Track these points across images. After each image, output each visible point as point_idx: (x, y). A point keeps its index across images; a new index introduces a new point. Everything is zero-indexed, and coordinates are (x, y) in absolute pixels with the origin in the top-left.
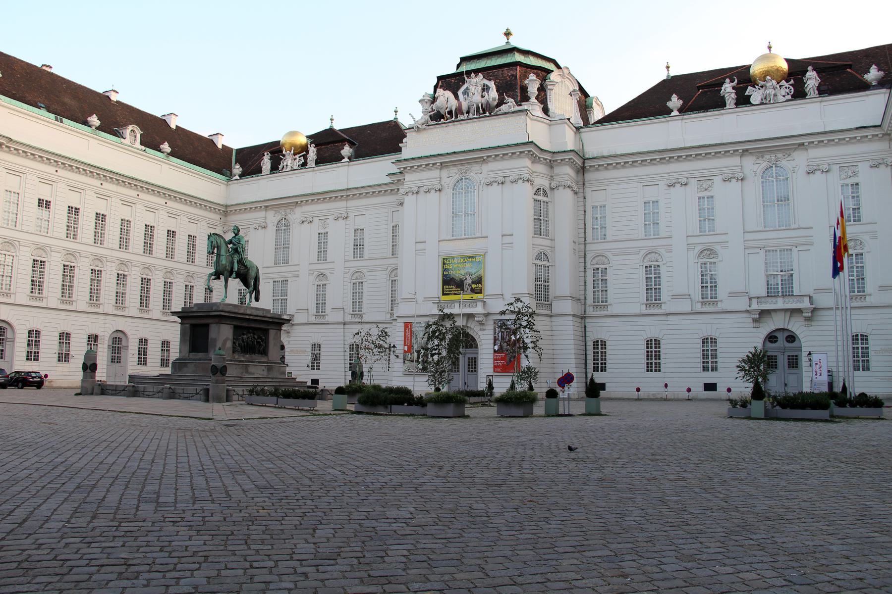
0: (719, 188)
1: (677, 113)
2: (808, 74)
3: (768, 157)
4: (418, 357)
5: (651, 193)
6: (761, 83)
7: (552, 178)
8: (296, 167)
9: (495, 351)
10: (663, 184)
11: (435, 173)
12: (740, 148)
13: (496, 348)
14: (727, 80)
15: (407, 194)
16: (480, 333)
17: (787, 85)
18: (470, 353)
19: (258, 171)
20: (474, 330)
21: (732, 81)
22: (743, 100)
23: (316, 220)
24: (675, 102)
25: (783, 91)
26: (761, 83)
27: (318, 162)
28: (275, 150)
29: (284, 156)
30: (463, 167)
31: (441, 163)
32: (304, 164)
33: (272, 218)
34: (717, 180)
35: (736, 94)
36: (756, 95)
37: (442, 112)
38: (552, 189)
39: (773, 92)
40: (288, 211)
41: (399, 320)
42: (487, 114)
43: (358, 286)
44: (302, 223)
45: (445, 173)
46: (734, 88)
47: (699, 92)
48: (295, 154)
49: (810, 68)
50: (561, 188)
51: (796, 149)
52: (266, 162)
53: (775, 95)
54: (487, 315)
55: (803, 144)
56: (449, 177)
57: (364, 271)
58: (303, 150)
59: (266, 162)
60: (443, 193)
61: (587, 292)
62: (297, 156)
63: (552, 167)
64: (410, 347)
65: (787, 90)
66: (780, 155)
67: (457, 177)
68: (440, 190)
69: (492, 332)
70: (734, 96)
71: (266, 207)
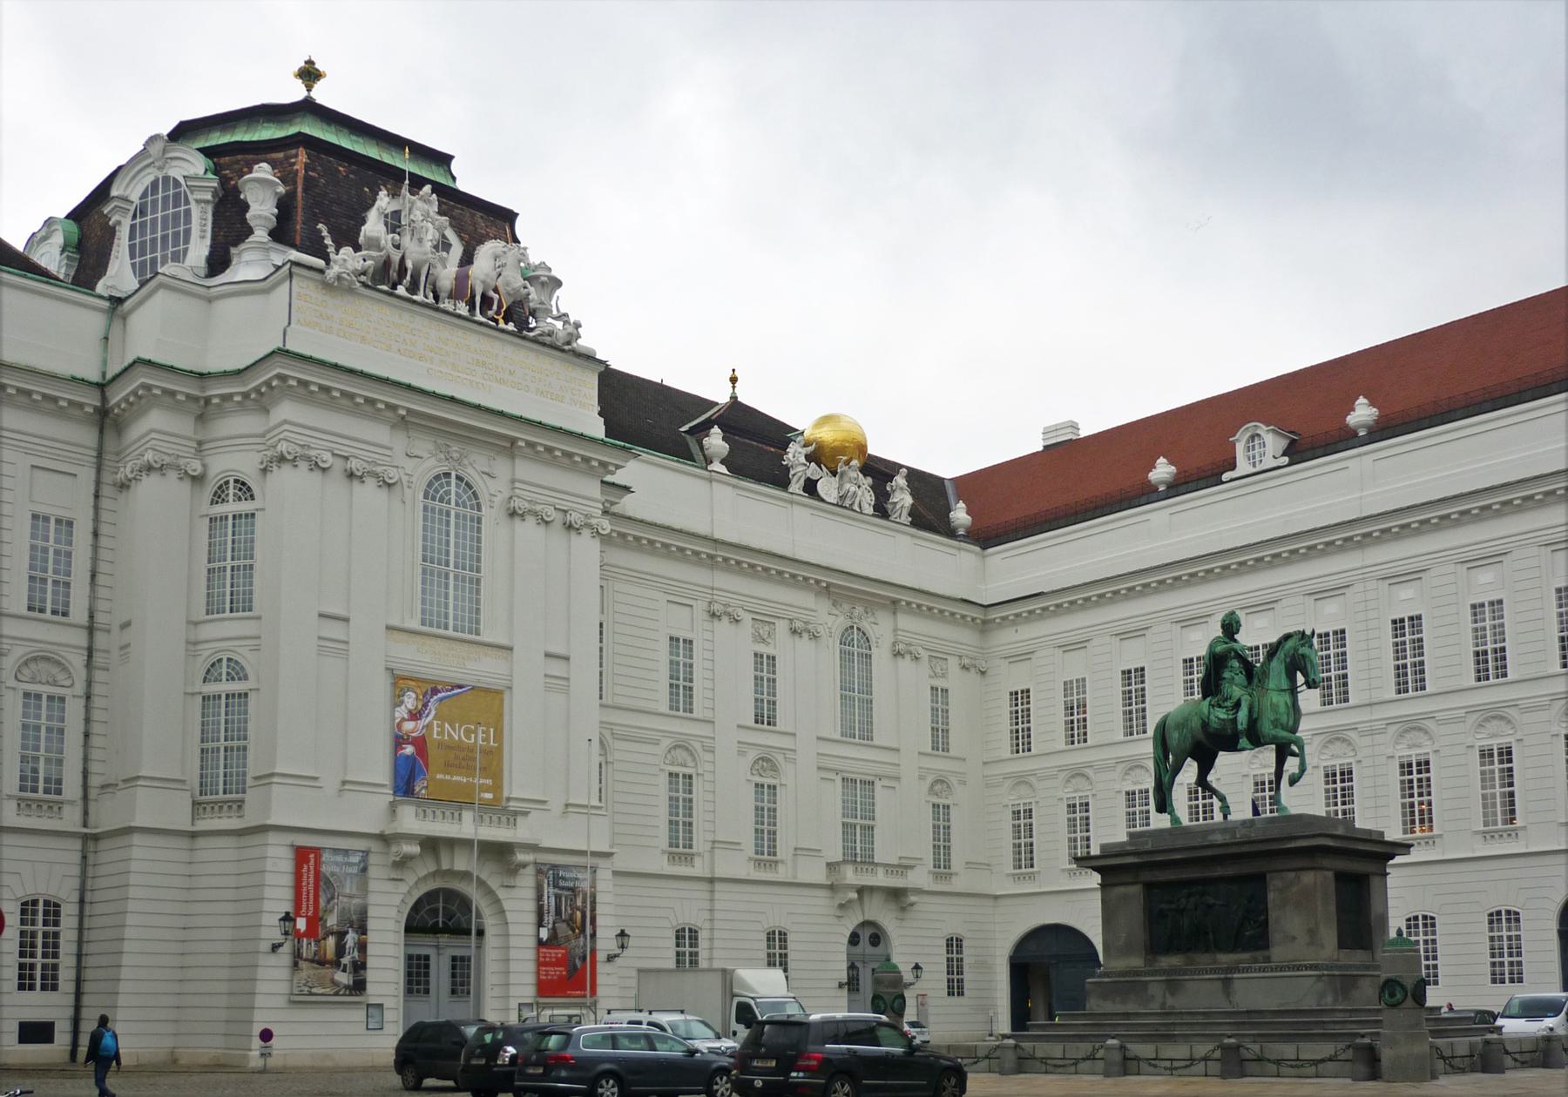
1: (723, 469)
4: (340, 950)
5: (680, 623)
9: (540, 943)
10: (700, 607)
12: (826, 578)
16: (501, 894)
22: (810, 487)
30: (455, 447)
41: (272, 838)
45: (398, 442)
51: (884, 606)
56: (416, 461)
64: (314, 922)
69: (530, 894)
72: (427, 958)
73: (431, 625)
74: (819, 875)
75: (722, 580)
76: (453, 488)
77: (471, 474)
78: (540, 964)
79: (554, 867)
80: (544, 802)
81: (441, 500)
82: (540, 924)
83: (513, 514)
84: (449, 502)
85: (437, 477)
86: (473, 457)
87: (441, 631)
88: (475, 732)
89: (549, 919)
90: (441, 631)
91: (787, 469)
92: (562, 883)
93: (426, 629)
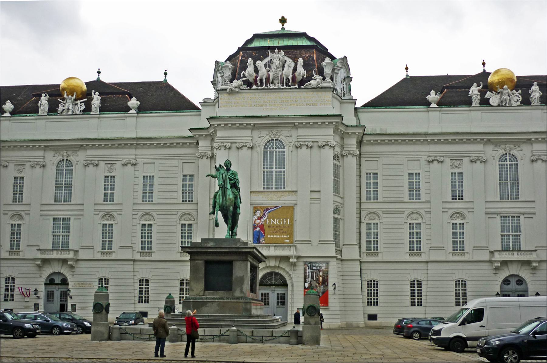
0: (466, 167)
1: (436, 106)
2: (533, 88)
3: (503, 146)
6: (499, 90)
7: (342, 147)
8: (78, 112)
9: (305, 288)
11: (248, 133)
12: (486, 137)
13: (307, 285)
14: (475, 84)
15: (219, 148)
16: (290, 273)
17: (517, 93)
18: (280, 290)
19: (35, 110)
20: (284, 270)
21: (478, 86)
22: (485, 102)
23: (102, 164)
24: (433, 96)
25: (516, 98)
26: (499, 90)
27: (103, 109)
28: (55, 93)
29: (64, 99)
30: (274, 131)
31: (254, 124)
32: (88, 109)
33: (52, 158)
34: (466, 161)
35: (481, 96)
36: (494, 99)
37: (251, 79)
38: (343, 156)
39: (509, 98)
40: (70, 153)
42: (297, 86)
43: (146, 229)
44: (86, 166)
45: (256, 134)
46: (479, 91)
47: (454, 91)
48: (76, 100)
49: (535, 83)
50: (350, 156)
51: (524, 142)
52: (44, 102)
53: (510, 101)
54: (298, 257)
55: (530, 139)
56: (261, 138)
57: (154, 214)
58: (85, 96)
59: (44, 102)
60: (254, 151)
61: (362, 242)
62: (78, 102)
63: (342, 138)
65: (517, 98)
66: (512, 146)
67: (268, 138)
68: (252, 148)
69: (303, 272)
70: (479, 97)
71: (46, 146)
72: (268, 294)
73: (267, 189)
74: (486, 257)
75: (433, 148)
76: (274, 144)
77: (282, 138)
78: (305, 295)
79: (310, 263)
80: (310, 241)
81: (270, 149)
82: (305, 282)
83: (297, 147)
84: (273, 149)
85: (269, 142)
86: (282, 132)
87: (271, 190)
88: (283, 221)
89: (309, 280)
90: (271, 190)
91: (471, 97)
92: (314, 268)
93: (265, 190)
